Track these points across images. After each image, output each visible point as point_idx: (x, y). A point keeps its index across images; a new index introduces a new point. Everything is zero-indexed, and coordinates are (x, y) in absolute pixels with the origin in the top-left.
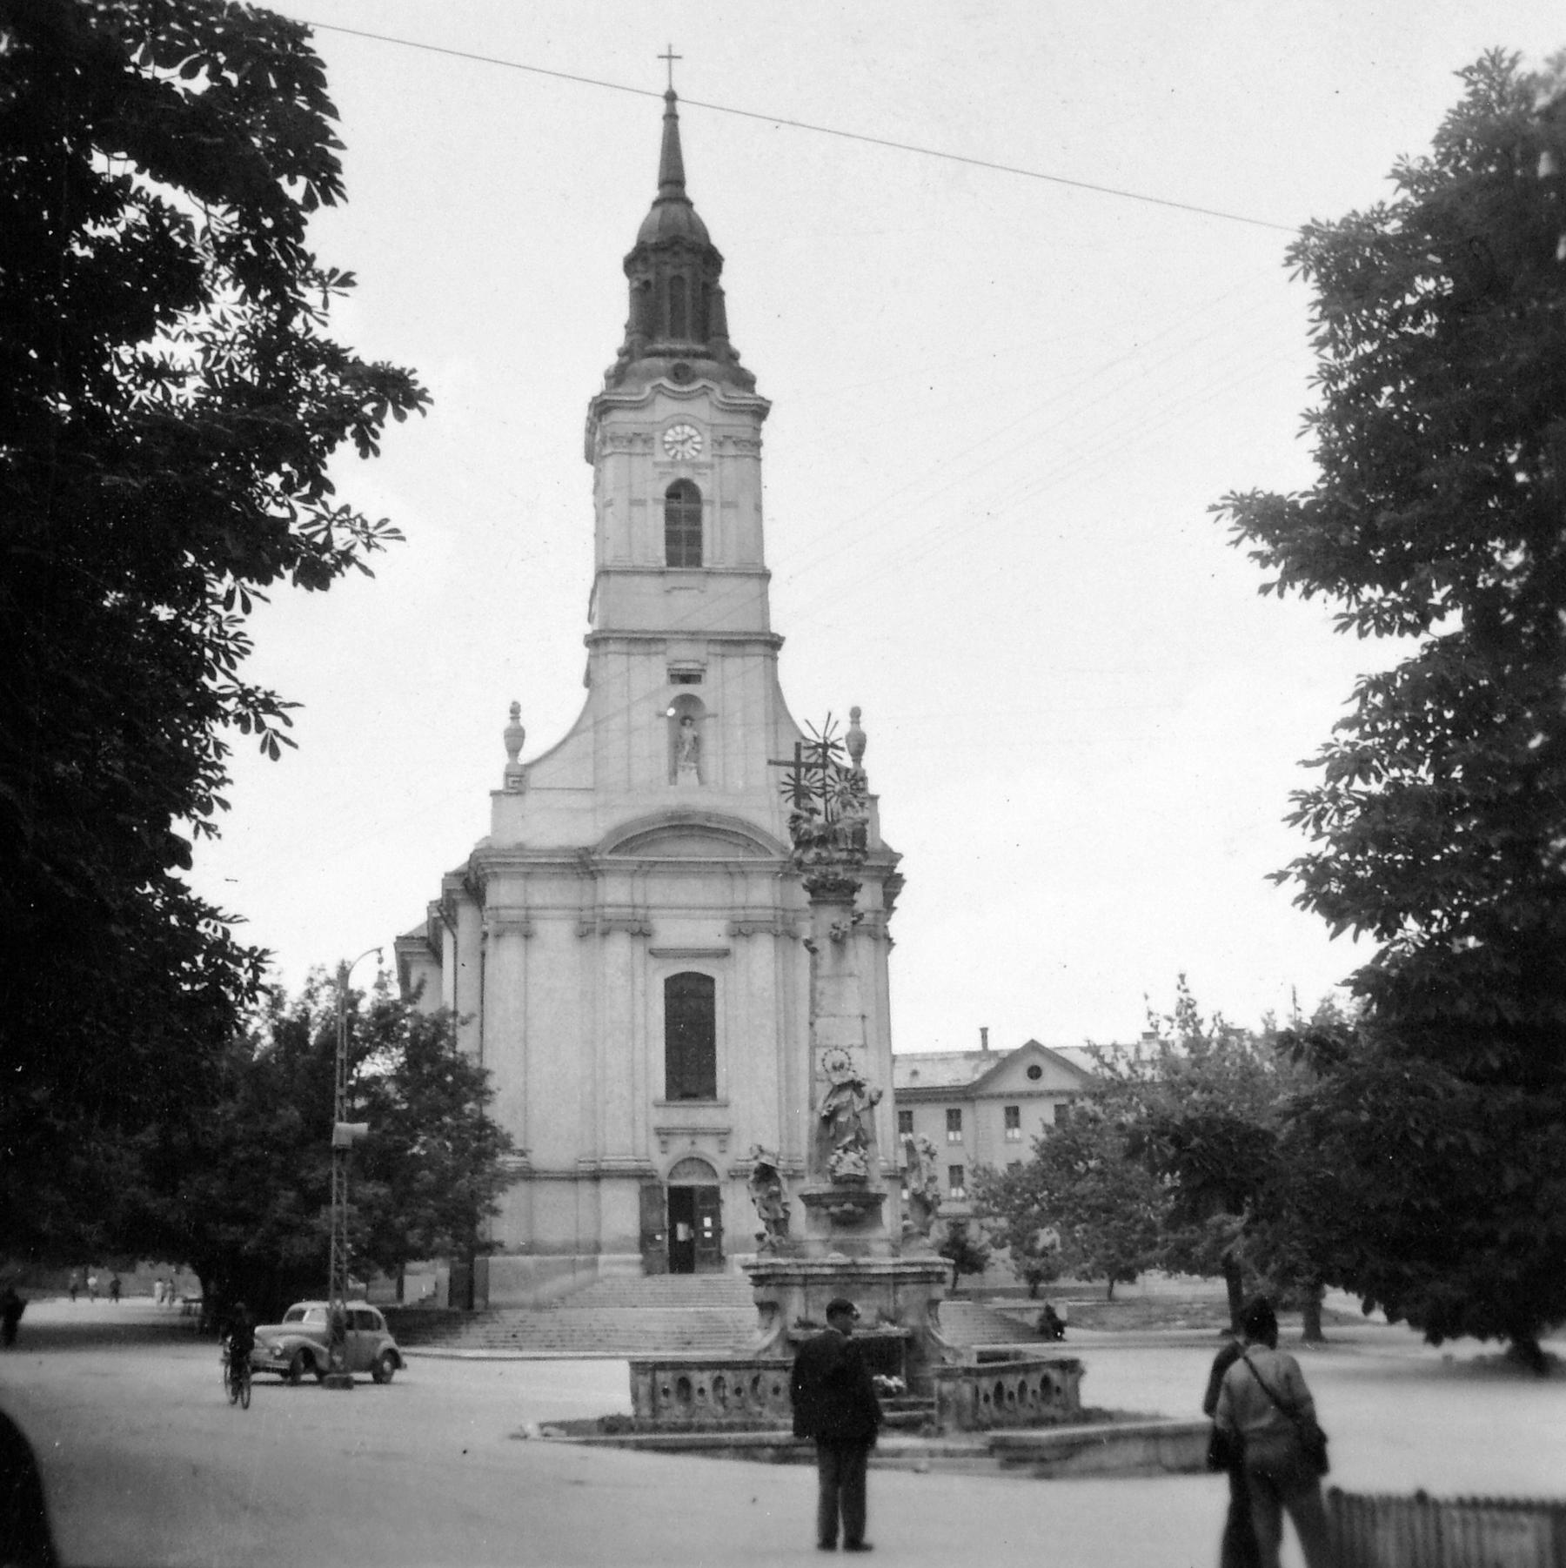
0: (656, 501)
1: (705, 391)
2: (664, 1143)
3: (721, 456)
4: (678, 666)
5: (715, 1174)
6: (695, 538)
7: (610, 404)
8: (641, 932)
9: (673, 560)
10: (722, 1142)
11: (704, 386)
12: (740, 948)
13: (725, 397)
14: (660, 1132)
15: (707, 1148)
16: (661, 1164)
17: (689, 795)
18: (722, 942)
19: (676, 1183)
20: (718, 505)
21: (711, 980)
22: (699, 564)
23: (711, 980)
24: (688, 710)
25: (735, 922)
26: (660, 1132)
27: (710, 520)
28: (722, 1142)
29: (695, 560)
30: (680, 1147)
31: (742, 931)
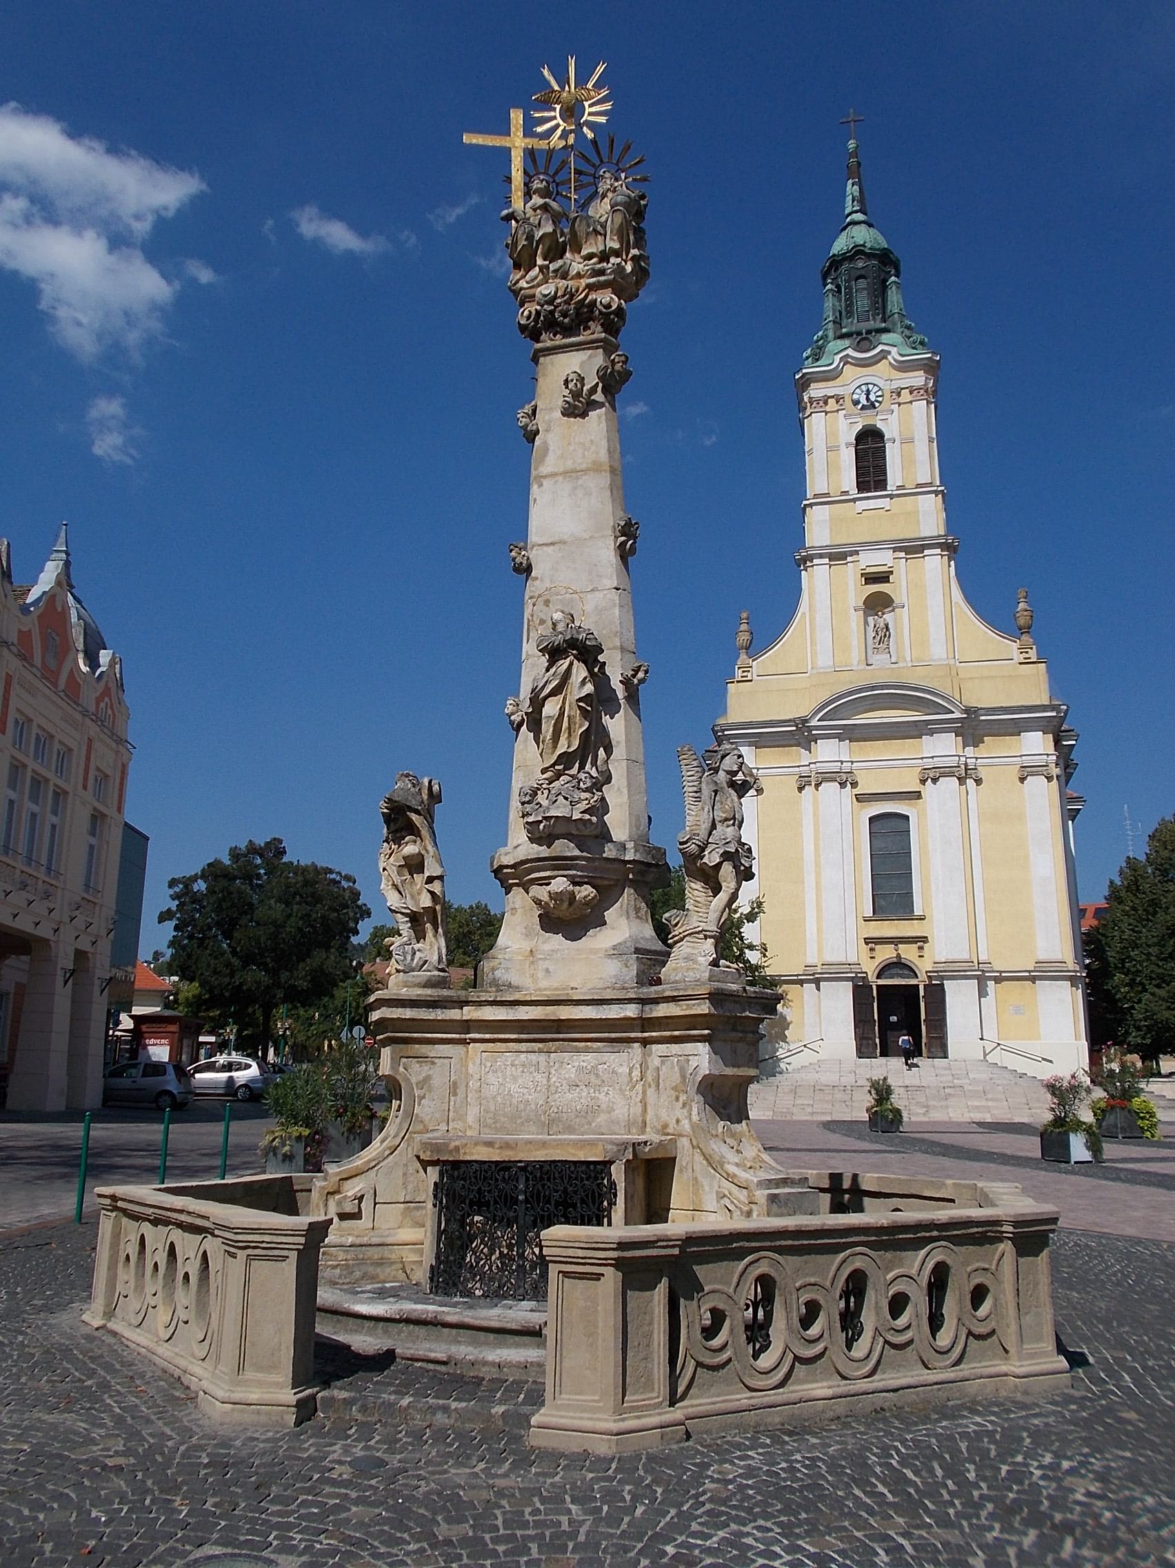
0: (848, 445)
2: (872, 949)
6: (881, 470)
7: (808, 376)
8: (845, 780)
9: (862, 486)
11: (882, 351)
12: (929, 789)
13: (901, 355)
14: (867, 941)
15: (908, 953)
16: (870, 968)
17: (882, 670)
19: (881, 982)
21: (907, 818)
23: (907, 818)
24: (877, 604)
26: (867, 941)
27: (892, 454)
28: (921, 948)
29: (881, 484)
30: (886, 953)
31: (932, 775)
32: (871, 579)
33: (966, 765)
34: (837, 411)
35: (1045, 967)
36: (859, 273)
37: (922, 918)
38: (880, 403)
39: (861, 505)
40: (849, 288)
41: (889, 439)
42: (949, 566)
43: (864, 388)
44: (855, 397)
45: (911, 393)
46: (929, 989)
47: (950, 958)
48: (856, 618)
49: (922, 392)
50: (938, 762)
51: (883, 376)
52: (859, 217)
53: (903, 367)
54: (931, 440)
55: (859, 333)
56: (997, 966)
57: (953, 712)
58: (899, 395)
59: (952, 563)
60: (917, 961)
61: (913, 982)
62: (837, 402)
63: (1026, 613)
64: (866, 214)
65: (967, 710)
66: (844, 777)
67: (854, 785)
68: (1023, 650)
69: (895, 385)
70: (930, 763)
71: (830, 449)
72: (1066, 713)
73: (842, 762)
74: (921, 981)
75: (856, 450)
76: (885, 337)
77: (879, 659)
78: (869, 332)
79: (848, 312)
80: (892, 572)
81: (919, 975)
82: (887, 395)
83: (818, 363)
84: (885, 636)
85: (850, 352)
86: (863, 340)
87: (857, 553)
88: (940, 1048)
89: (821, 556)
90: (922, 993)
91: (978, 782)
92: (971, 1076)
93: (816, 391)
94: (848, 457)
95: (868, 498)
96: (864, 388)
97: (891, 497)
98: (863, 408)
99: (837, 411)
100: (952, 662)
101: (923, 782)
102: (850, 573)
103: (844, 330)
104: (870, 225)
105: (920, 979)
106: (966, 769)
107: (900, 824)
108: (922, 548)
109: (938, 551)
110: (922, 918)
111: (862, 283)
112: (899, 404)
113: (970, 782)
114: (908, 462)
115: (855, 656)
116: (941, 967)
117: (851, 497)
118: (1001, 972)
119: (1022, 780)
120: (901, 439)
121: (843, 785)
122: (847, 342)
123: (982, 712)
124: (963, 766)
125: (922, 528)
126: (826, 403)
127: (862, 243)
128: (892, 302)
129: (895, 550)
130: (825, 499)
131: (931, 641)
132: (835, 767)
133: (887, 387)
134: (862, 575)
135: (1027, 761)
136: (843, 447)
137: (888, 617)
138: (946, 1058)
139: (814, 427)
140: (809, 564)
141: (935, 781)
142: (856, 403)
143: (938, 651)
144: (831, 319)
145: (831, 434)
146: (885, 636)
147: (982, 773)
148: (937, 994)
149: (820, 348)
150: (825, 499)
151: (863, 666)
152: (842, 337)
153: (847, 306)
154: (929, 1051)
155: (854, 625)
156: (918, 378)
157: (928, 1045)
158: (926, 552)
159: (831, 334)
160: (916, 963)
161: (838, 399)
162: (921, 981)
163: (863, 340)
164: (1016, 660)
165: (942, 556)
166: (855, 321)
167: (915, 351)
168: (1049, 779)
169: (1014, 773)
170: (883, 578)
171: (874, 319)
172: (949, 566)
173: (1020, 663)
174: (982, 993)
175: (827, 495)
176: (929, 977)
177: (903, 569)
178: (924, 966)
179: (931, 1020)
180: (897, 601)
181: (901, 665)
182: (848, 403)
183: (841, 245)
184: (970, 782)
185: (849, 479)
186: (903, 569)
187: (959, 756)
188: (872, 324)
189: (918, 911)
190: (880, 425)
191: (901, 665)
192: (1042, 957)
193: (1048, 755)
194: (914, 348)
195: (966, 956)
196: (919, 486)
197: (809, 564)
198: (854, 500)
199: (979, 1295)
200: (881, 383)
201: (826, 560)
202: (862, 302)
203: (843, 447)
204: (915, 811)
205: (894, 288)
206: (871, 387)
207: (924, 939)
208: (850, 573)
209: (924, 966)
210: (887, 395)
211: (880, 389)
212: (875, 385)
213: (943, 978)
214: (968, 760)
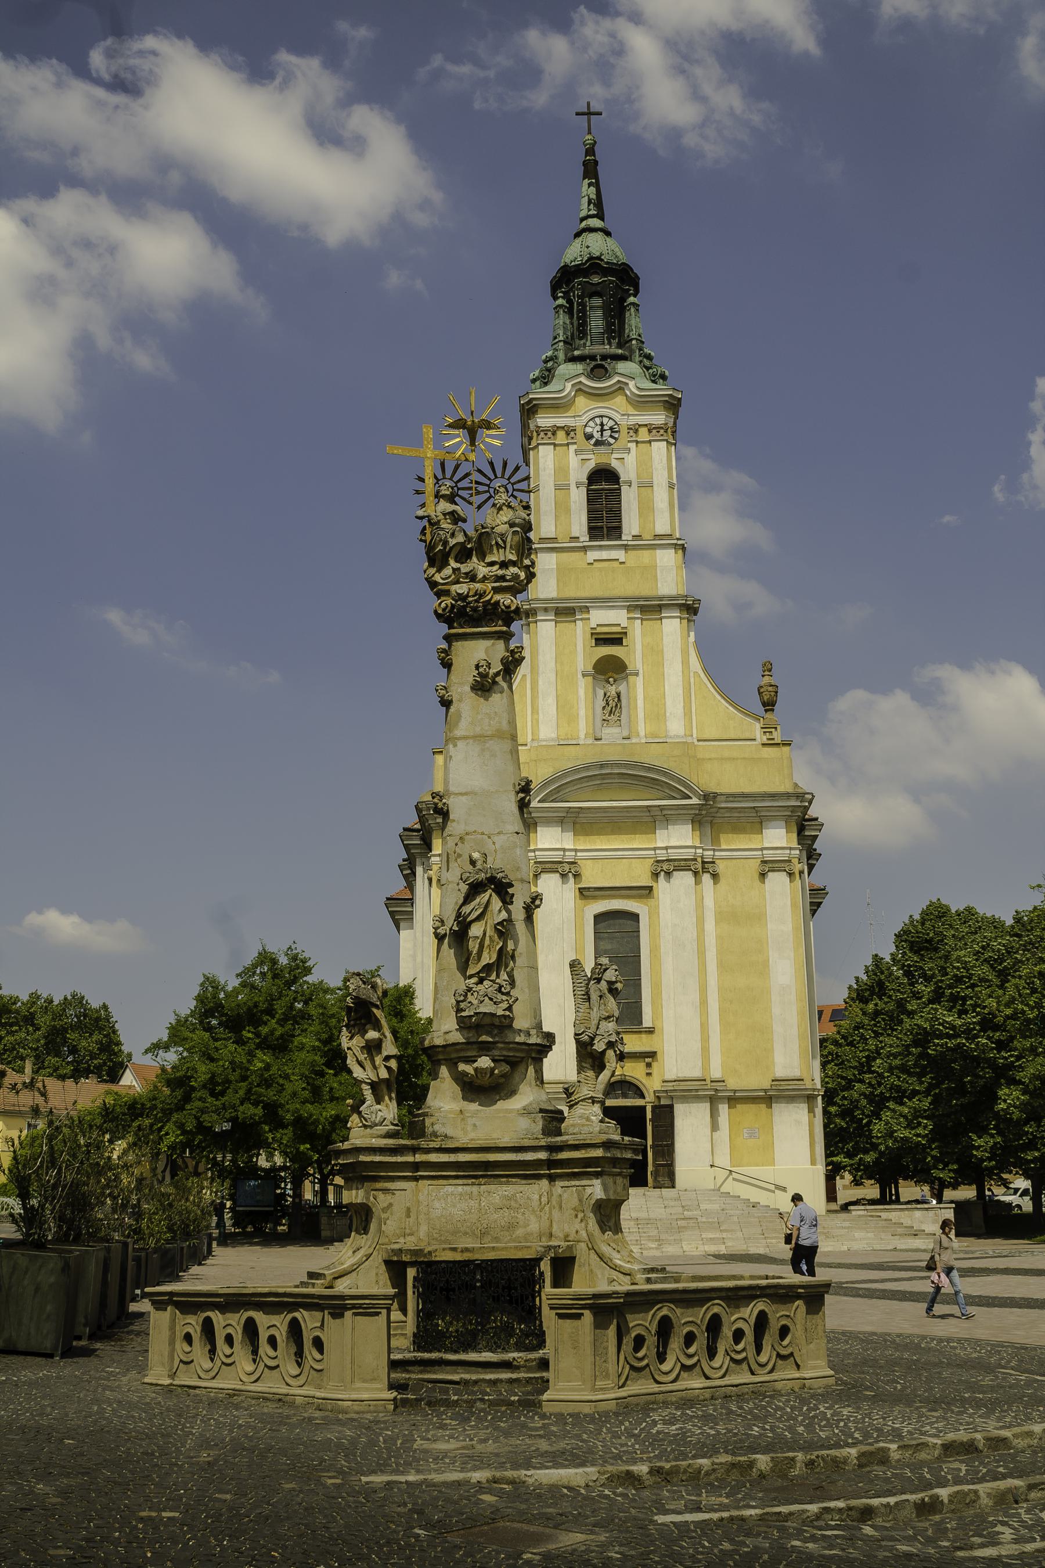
0: (578, 485)
1: (621, 388)
3: (637, 442)
4: (599, 630)
5: (642, 1096)
6: (616, 514)
10: (649, 1065)
11: (619, 381)
12: (662, 886)
15: (633, 1071)
18: (645, 881)
20: (634, 485)
21: (635, 917)
22: (620, 538)
25: (658, 861)
27: (629, 499)
28: (649, 1065)
32: (603, 640)
34: (568, 445)
35: (784, 1086)
36: (594, 289)
37: (651, 1031)
38: (616, 439)
39: (592, 555)
40: (583, 305)
41: (625, 482)
43: (598, 421)
44: (588, 430)
45: (650, 431)
46: (657, 1111)
47: (681, 1075)
48: (583, 687)
49: (662, 432)
50: (674, 854)
51: (618, 410)
52: (595, 223)
53: (641, 402)
54: (671, 486)
55: (593, 358)
56: (732, 1083)
57: (690, 798)
58: (636, 431)
60: (644, 1080)
61: (639, 1102)
62: (568, 434)
63: (770, 689)
64: (602, 219)
65: (706, 797)
66: (567, 868)
67: (577, 876)
68: (767, 729)
69: (633, 420)
70: (662, 855)
71: (558, 488)
72: (810, 802)
73: (564, 850)
74: (648, 1102)
75: (588, 490)
76: (622, 366)
77: (611, 733)
78: (604, 357)
79: (580, 332)
80: (626, 633)
81: (646, 1095)
82: (624, 431)
83: (546, 389)
84: (617, 705)
85: (583, 379)
86: (599, 368)
87: (587, 610)
88: (667, 1176)
89: (546, 610)
90: (649, 1115)
91: (715, 876)
92: (703, 1206)
93: (543, 420)
94: (578, 498)
95: (601, 547)
96: (598, 421)
97: (626, 547)
98: (598, 443)
99: (568, 445)
101: (656, 875)
102: (579, 632)
103: (576, 353)
104: (608, 234)
105: (647, 1099)
106: (703, 862)
107: (629, 924)
108: (660, 608)
110: (651, 1031)
111: (597, 301)
112: (637, 442)
113: (706, 878)
114: (646, 509)
115: (582, 729)
116: (670, 1086)
117: (581, 545)
118: (735, 1091)
119: (763, 875)
120: (639, 483)
121: (564, 876)
122: (579, 368)
123: (723, 798)
124: (699, 860)
125: (659, 585)
126: (554, 434)
127: (598, 254)
128: (630, 326)
129: (630, 609)
130: (553, 546)
132: (556, 856)
133: (624, 422)
134: (592, 634)
135: (769, 855)
136: (573, 487)
137: (622, 688)
138: (673, 1187)
139: (541, 461)
141: (668, 874)
142: (589, 437)
143: (675, 727)
144: (561, 338)
145: (561, 470)
146: (617, 705)
147: (721, 867)
148: (665, 1114)
149: (549, 370)
150: (553, 546)
151: (590, 741)
152: (573, 359)
153: (579, 325)
154: (655, 1180)
155: (582, 692)
156: (659, 418)
157: (656, 1174)
159: (561, 356)
160: (644, 1081)
161: (569, 431)
162: (648, 1102)
163: (599, 368)
164: (759, 741)
165: (681, 618)
166: (588, 343)
167: (654, 386)
168: (791, 875)
169: (755, 866)
170: (616, 640)
171: (610, 344)
173: (764, 745)
174: (714, 1114)
175: (554, 540)
176: (659, 1098)
177: (638, 631)
178: (652, 1085)
179: (658, 1146)
180: (631, 668)
181: (634, 741)
182: (580, 437)
183: (574, 253)
184: (706, 878)
185: (579, 524)
186: (638, 631)
188: (606, 349)
189: (647, 1022)
190: (615, 464)
191: (634, 741)
192: (780, 1073)
193: (791, 849)
194: (654, 382)
195: (697, 1073)
196: (657, 537)
198: (585, 549)
199: (784, 1331)
200: (617, 417)
202: (596, 321)
203: (573, 487)
204: (646, 909)
205: (632, 310)
206: (605, 420)
207: (653, 1055)
208: (579, 632)
209: (652, 1085)
210: (624, 431)
211: (616, 423)
212: (610, 418)
213: (672, 1098)
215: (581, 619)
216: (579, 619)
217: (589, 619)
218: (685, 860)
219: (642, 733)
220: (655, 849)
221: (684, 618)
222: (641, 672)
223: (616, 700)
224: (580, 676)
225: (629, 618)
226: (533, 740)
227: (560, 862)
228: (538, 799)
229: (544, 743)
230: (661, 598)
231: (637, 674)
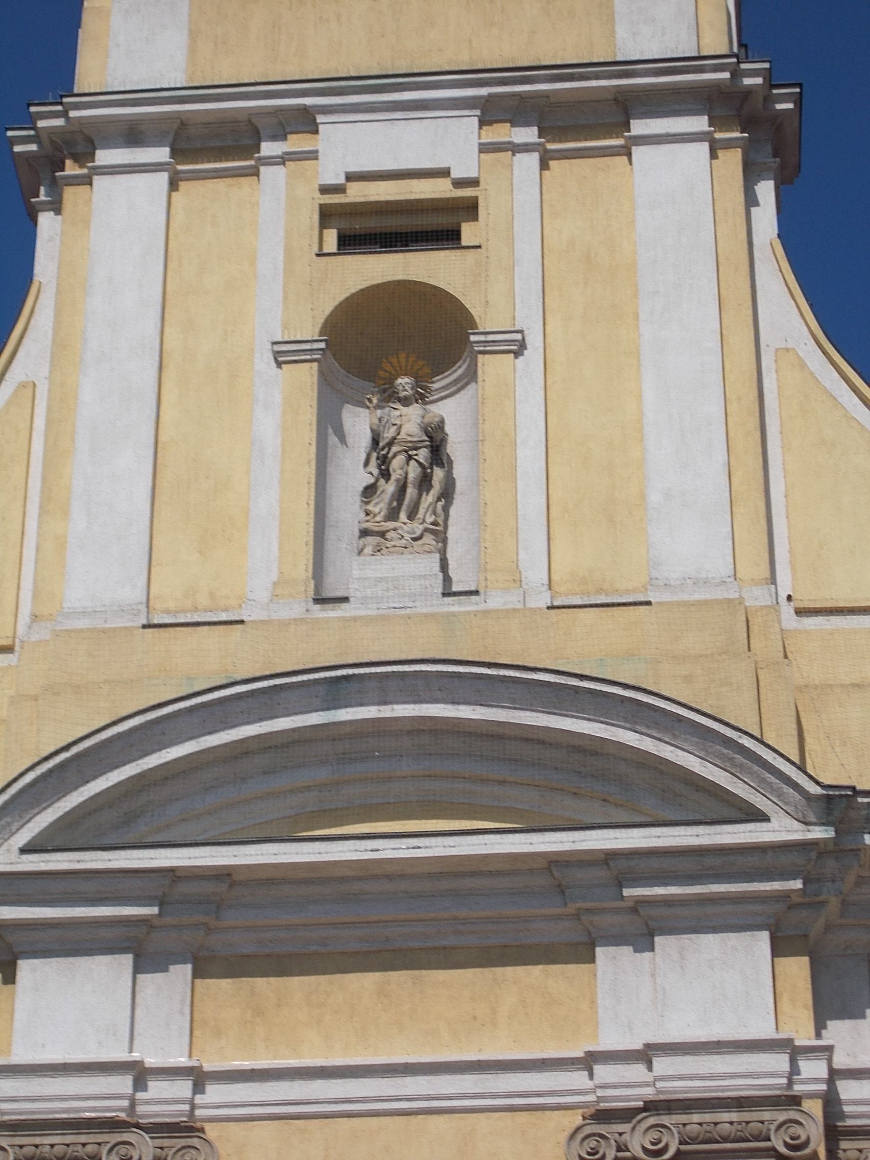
4: (358, 193)
33: (831, 1101)
42: (751, 200)
57: (762, 817)
59: (766, 190)
80: (470, 209)
84: (425, 482)
100: (757, 597)
109: (700, 123)
124: (815, 1108)
131: (654, 498)
134: (327, 215)
140: (71, 169)
146: (425, 482)
158: (639, 127)
172: (751, 200)
181: (495, 601)
187: (795, 1052)
191: (495, 601)
197: (71, 169)
201: (161, 154)
214: (848, 1090)
215: (283, 160)
216: (270, 161)
217: (313, 155)
218: (740, 1103)
219: (536, 575)
220: (589, 1061)
221: (728, 144)
222: (534, 341)
223: (423, 455)
224: (264, 361)
225: (485, 148)
226: (35, 617)
227: (113, 1125)
228: (24, 837)
229: (83, 623)
230: (626, 67)
231: (519, 349)
